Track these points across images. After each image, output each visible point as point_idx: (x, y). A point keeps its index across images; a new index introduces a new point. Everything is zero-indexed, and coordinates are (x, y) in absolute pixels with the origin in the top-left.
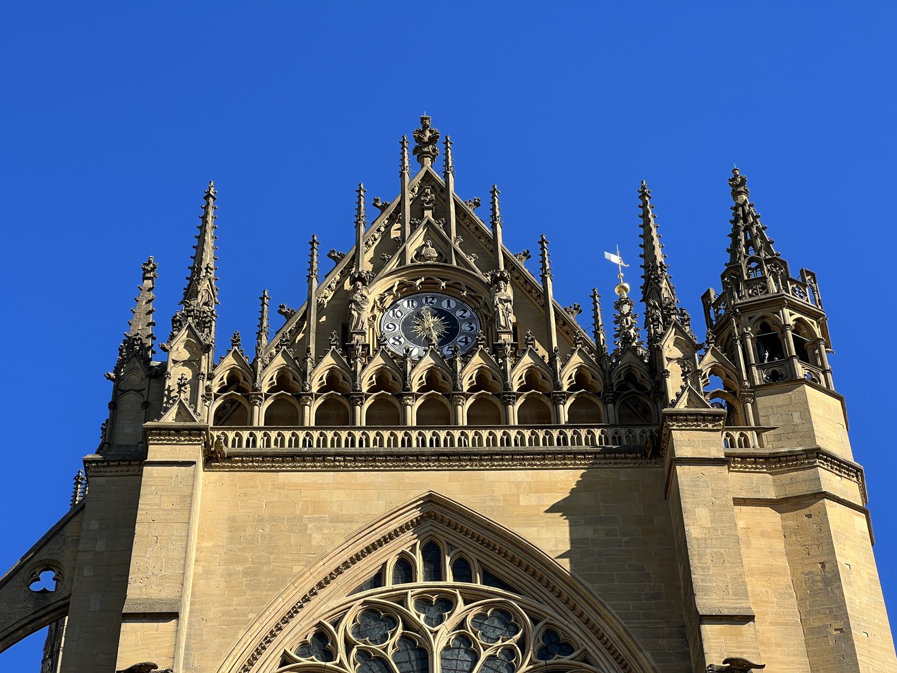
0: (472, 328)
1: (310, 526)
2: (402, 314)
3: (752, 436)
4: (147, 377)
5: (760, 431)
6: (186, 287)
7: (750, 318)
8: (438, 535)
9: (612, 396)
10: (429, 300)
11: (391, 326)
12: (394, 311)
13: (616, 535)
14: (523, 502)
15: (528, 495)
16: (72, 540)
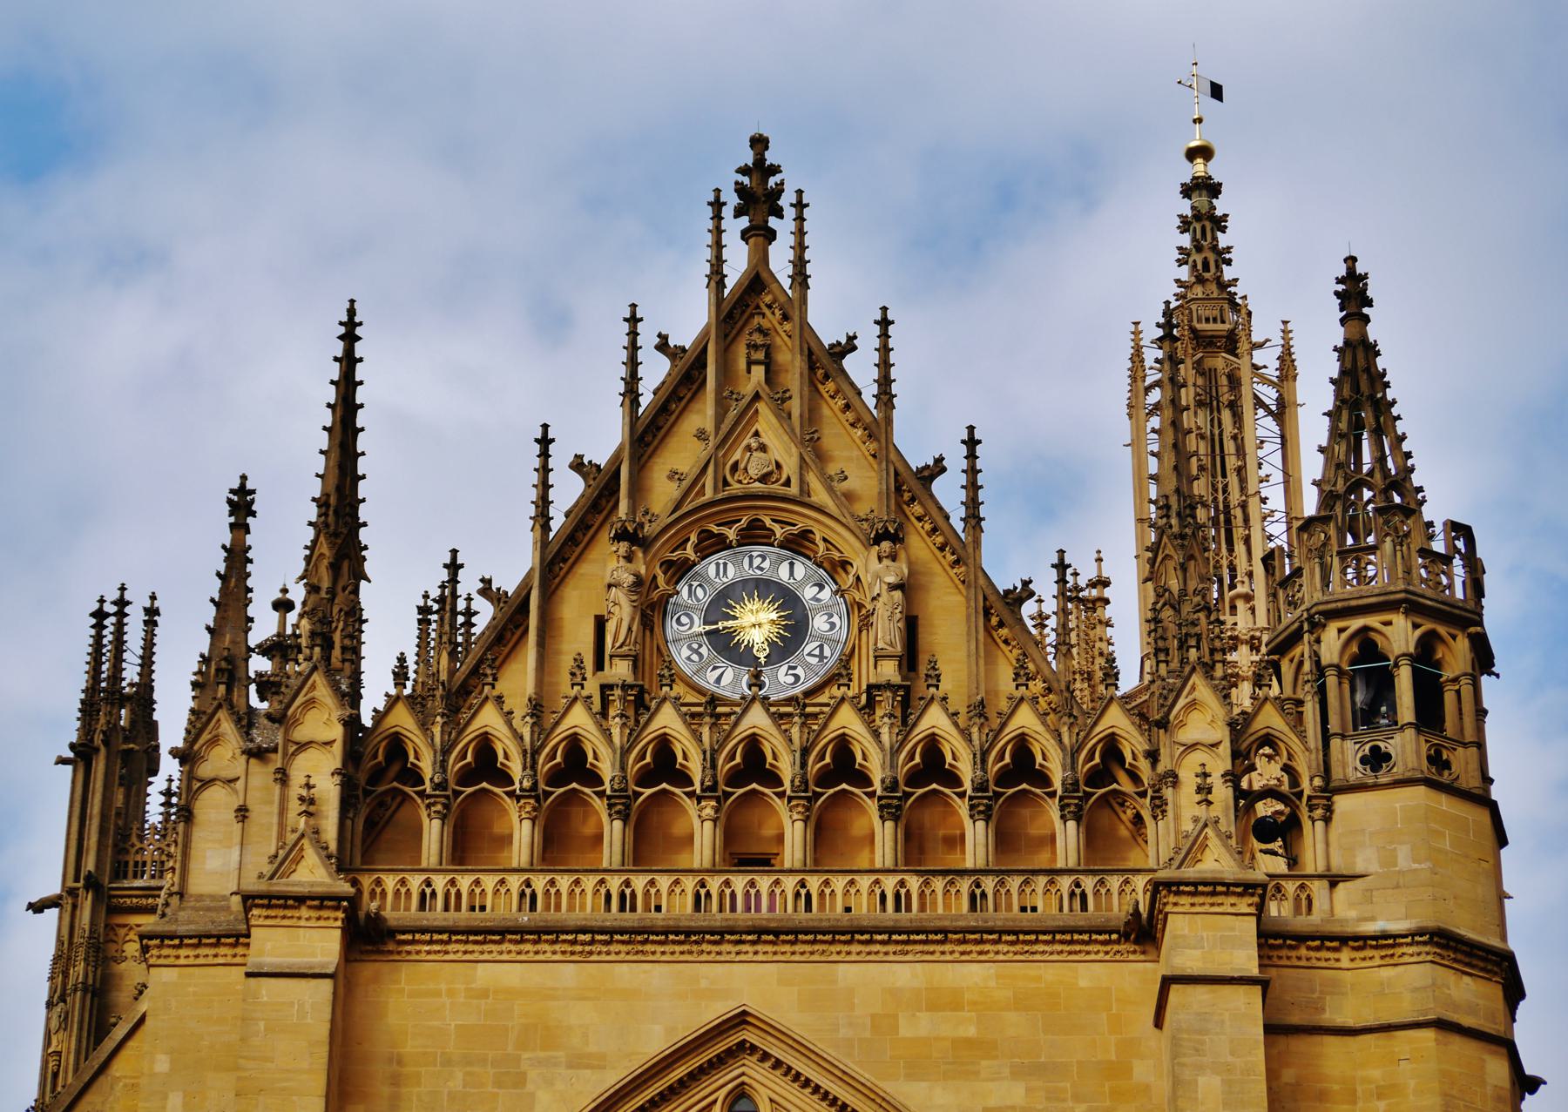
0: (833, 625)
1: (532, 1074)
2: (705, 594)
3: (1318, 889)
4: (243, 752)
5: (1334, 881)
6: (309, 544)
7: (1341, 631)
8: (755, 1085)
9: (1076, 805)
10: (757, 562)
11: (684, 620)
12: (691, 586)
13: (1064, 1100)
14: (905, 1031)
15: (914, 1015)
16: (125, 1085)
